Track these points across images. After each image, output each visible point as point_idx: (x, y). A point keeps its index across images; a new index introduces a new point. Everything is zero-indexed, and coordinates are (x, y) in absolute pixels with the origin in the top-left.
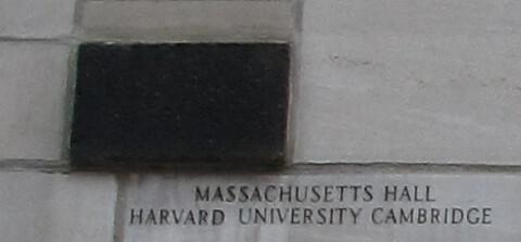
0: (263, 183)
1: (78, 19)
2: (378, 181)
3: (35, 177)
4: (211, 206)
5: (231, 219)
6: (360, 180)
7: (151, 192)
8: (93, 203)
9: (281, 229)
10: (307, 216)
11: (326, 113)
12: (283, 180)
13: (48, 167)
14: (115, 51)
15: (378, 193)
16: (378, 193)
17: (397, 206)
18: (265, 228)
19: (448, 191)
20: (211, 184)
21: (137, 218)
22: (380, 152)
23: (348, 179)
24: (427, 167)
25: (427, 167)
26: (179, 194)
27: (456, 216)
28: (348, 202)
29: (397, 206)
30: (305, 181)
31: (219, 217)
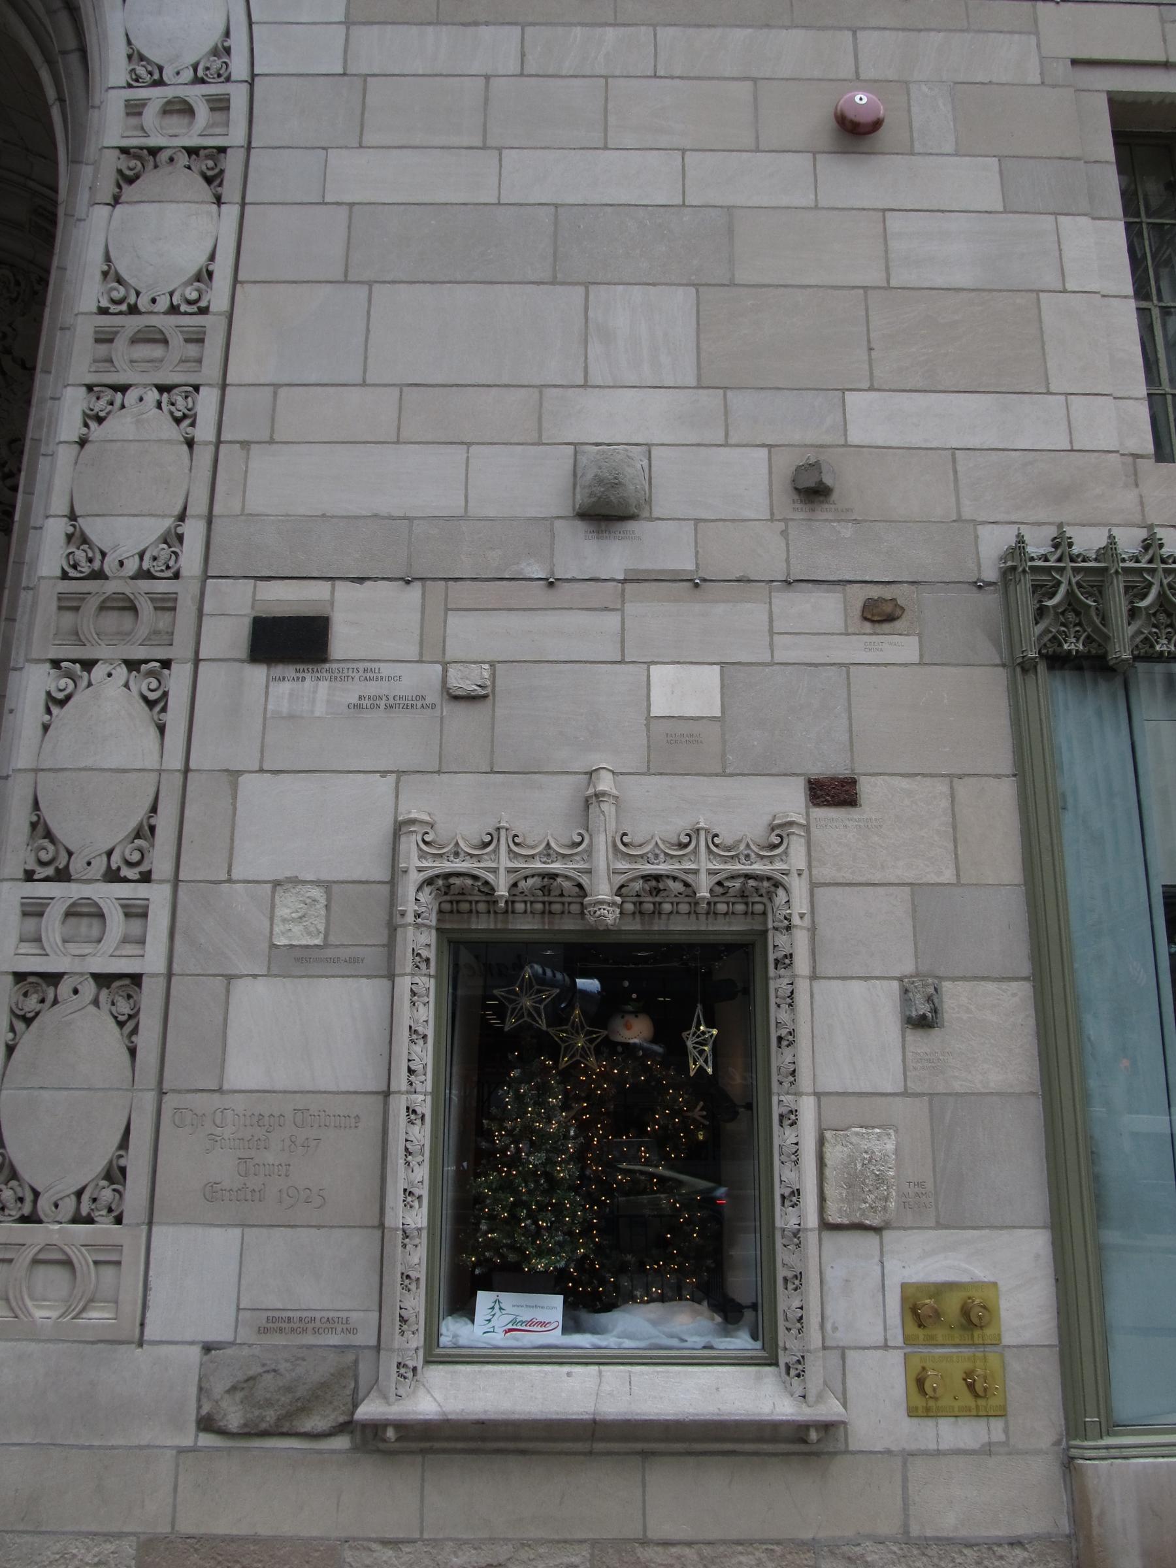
0: (319, 666)
1: (253, 608)
2: (361, 666)
3: (237, 664)
4: (300, 675)
5: (308, 680)
6: (355, 665)
7: (279, 670)
8: (259, 673)
9: (326, 683)
10: (336, 678)
11: (341, 643)
12: (327, 666)
13: (242, 661)
14: (266, 619)
15: (361, 670)
16: (361, 670)
17: (368, 675)
18: (321, 683)
19: (386, 670)
20: (300, 667)
21: (274, 679)
22: (362, 656)
23: (350, 665)
24: (379, 661)
25: (379, 661)
26: (289, 670)
27: (389, 678)
28: (350, 674)
29: (368, 675)
30: (335, 666)
31: (304, 679)
